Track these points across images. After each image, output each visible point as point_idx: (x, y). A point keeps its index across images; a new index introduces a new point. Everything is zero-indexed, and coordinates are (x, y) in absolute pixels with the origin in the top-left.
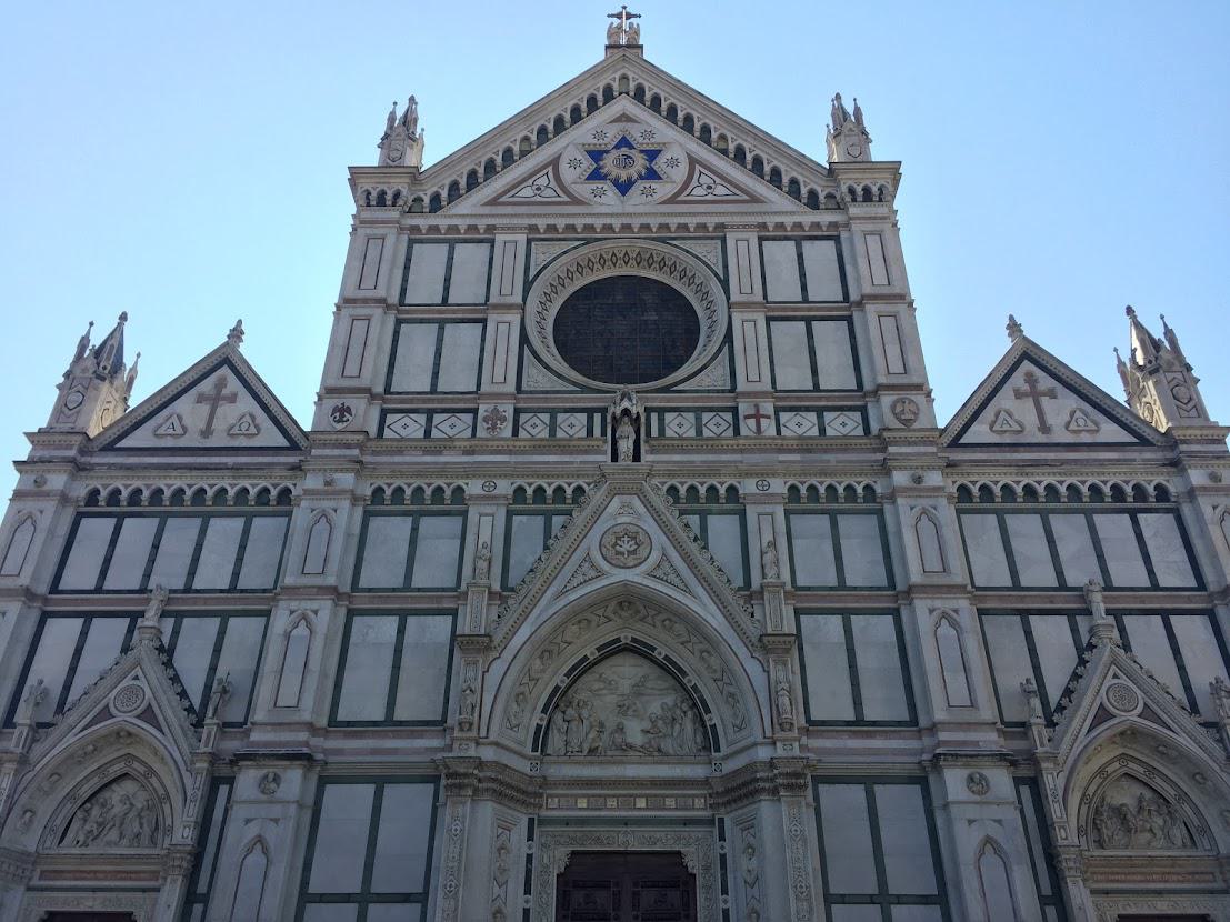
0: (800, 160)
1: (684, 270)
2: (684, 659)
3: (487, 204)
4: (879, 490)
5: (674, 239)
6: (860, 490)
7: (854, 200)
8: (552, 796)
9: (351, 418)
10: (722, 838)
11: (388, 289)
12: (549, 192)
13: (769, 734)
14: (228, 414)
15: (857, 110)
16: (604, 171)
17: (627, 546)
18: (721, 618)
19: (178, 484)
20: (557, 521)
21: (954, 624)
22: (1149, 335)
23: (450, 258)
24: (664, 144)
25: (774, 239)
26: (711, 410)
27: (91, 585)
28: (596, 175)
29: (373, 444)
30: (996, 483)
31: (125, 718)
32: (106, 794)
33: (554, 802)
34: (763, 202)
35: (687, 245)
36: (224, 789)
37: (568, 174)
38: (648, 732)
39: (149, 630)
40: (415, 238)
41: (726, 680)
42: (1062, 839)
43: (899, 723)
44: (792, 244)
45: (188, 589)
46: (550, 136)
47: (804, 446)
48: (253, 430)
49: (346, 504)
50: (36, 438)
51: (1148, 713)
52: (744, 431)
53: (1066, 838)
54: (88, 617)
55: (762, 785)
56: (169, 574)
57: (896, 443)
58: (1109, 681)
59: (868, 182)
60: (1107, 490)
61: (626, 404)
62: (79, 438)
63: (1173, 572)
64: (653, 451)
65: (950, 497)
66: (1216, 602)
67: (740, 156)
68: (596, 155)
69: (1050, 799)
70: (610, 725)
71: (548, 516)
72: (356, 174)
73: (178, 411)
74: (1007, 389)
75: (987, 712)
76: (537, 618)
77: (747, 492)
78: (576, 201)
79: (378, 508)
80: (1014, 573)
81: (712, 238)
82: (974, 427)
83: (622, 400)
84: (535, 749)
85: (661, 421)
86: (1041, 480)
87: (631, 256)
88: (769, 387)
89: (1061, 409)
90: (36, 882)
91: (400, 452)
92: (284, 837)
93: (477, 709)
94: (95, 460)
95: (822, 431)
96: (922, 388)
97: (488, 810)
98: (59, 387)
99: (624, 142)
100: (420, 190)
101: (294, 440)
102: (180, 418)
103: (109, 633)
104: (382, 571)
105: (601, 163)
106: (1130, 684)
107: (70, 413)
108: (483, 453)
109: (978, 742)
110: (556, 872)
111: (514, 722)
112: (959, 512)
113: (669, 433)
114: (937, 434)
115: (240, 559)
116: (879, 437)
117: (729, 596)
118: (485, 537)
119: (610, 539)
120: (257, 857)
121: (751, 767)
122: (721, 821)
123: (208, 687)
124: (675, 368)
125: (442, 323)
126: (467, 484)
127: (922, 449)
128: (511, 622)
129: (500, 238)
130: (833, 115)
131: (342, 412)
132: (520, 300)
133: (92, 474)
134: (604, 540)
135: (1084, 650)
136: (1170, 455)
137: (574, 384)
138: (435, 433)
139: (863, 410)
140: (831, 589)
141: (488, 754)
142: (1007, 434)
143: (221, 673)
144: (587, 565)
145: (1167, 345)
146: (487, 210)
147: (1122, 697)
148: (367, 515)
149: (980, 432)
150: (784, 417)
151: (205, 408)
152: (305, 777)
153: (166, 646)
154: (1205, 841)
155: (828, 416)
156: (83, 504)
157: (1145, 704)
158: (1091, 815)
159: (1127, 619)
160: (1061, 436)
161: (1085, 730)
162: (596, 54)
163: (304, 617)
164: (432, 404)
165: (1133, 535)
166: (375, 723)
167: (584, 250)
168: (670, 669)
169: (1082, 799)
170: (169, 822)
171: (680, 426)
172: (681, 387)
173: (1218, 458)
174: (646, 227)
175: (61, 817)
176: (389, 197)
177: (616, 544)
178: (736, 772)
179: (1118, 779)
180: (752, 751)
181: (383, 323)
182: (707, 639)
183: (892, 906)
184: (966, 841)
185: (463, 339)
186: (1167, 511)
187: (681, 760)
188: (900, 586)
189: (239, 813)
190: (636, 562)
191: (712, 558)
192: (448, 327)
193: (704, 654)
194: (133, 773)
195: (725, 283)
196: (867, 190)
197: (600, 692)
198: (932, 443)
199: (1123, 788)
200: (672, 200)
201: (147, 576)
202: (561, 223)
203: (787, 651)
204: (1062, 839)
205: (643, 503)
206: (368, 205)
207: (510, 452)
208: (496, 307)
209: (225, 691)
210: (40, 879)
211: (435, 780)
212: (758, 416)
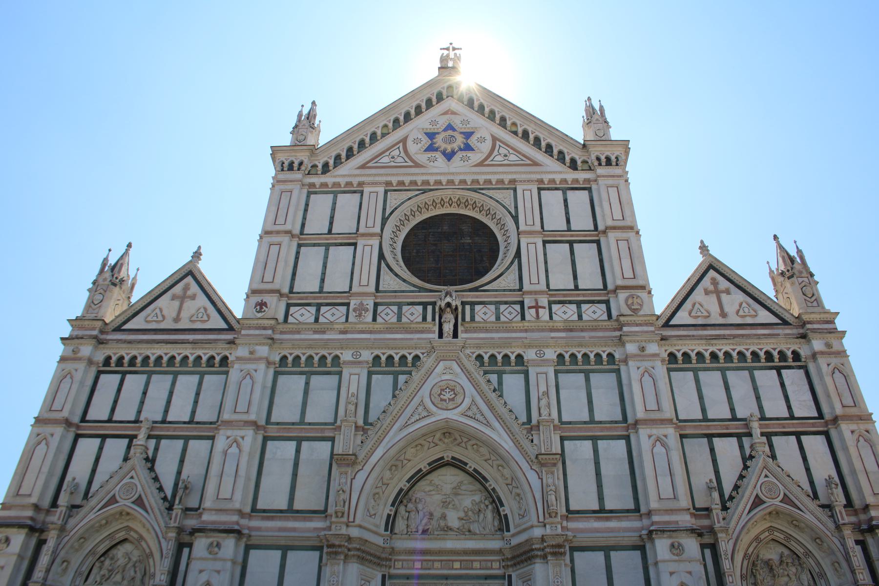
0: (565, 138)
1: (489, 209)
3: (359, 168)
5: (482, 189)
6: (604, 356)
7: (600, 164)
8: (399, 560)
11: (293, 224)
12: (400, 160)
13: (541, 519)
14: (190, 307)
15: (602, 108)
16: (436, 145)
17: (448, 395)
18: (511, 444)
19: (159, 352)
20: (402, 378)
22: (788, 254)
23: (334, 203)
24: (476, 128)
25: (548, 189)
26: (506, 303)
27: (106, 418)
28: (431, 148)
29: (280, 327)
30: (692, 351)
31: (125, 503)
33: (399, 565)
34: (541, 165)
35: (490, 193)
36: (186, 551)
37: (412, 148)
38: (462, 519)
39: (141, 447)
41: (514, 484)
42: (730, 583)
43: (628, 511)
45: (164, 421)
48: (205, 318)
49: (262, 366)
50: (74, 323)
51: (786, 500)
52: (527, 317)
53: (733, 582)
54: (104, 437)
55: (536, 553)
56: (153, 411)
58: (762, 479)
59: (608, 153)
60: (762, 354)
61: (448, 299)
62: (100, 323)
63: (803, 407)
64: (466, 331)
65: (663, 361)
66: (829, 426)
67: (525, 135)
68: (431, 136)
69: (723, 557)
70: (437, 514)
71: (396, 375)
72: (275, 151)
74: (700, 289)
75: (684, 502)
76: (387, 444)
77: (530, 358)
78: (417, 165)
79: (283, 369)
80: (704, 410)
81: (508, 189)
82: (679, 314)
83: (446, 296)
84: (386, 530)
86: (721, 348)
87: (453, 200)
88: (544, 288)
89: (734, 300)
91: (299, 332)
93: (347, 504)
94: (109, 337)
95: (580, 317)
96: (644, 288)
97: (354, 569)
98: (89, 290)
99: (450, 127)
100: (317, 160)
101: (231, 326)
102: (161, 310)
103: (115, 448)
105: (434, 140)
106: (775, 481)
109: (677, 521)
111: (372, 512)
112: (669, 370)
113: (477, 318)
114: (655, 318)
115: (196, 402)
116: (617, 320)
117: (516, 428)
118: (353, 389)
119: (437, 390)
122: (510, 577)
123: (176, 485)
125: (327, 246)
126: (342, 354)
127: (645, 328)
128: (370, 446)
129: (367, 190)
130: (586, 110)
131: (262, 305)
132: (377, 229)
133: (107, 346)
134: (433, 391)
135: (747, 459)
136: (801, 331)
137: (414, 286)
138: (321, 319)
139: (607, 302)
140: (585, 423)
141: (354, 532)
142: (700, 318)
143: (184, 476)
145: (798, 260)
146: (358, 172)
147: (770, 490)
148: (277, 374)
149: (682, 318)
150: (555, 307)
151: (177, 303)
152: (237, 545)
155: (584, 307)
156: (101, 365)
159: (774, 439)
163: (236, 441)
165: (778, 384)
166: (281, 511)
167: (423, 197)
168: (478, 477)
169: (744, 557)
171: (485, 313)
173: (830, 333)
174: (464, 182)
177: (441, 394)
178: (519, 545)
180: (531, 530)
181: (289, 246)
185: (341, 256)
186: (800, 367)
187: (484, 537)
188: (630, 420)
189: (195, 566)
190: (454, 406)
191: (505, 403)
192: (332, 249)
193: (500, 468)
194: (131, 538)
195: (516, 219)
196: (608, 160)
197: (430, 493)
198: (651, 324)
199: (771, 549)
200: (481, 164)
201: (139, 412)
202: (407, 180)
204: (730, 583)
205: (459, 366)
206: (282, 170)
207: (371, 332)
208: (363, 235)
209: (186, 488)
211: (320, 548)
212: (537, 307)
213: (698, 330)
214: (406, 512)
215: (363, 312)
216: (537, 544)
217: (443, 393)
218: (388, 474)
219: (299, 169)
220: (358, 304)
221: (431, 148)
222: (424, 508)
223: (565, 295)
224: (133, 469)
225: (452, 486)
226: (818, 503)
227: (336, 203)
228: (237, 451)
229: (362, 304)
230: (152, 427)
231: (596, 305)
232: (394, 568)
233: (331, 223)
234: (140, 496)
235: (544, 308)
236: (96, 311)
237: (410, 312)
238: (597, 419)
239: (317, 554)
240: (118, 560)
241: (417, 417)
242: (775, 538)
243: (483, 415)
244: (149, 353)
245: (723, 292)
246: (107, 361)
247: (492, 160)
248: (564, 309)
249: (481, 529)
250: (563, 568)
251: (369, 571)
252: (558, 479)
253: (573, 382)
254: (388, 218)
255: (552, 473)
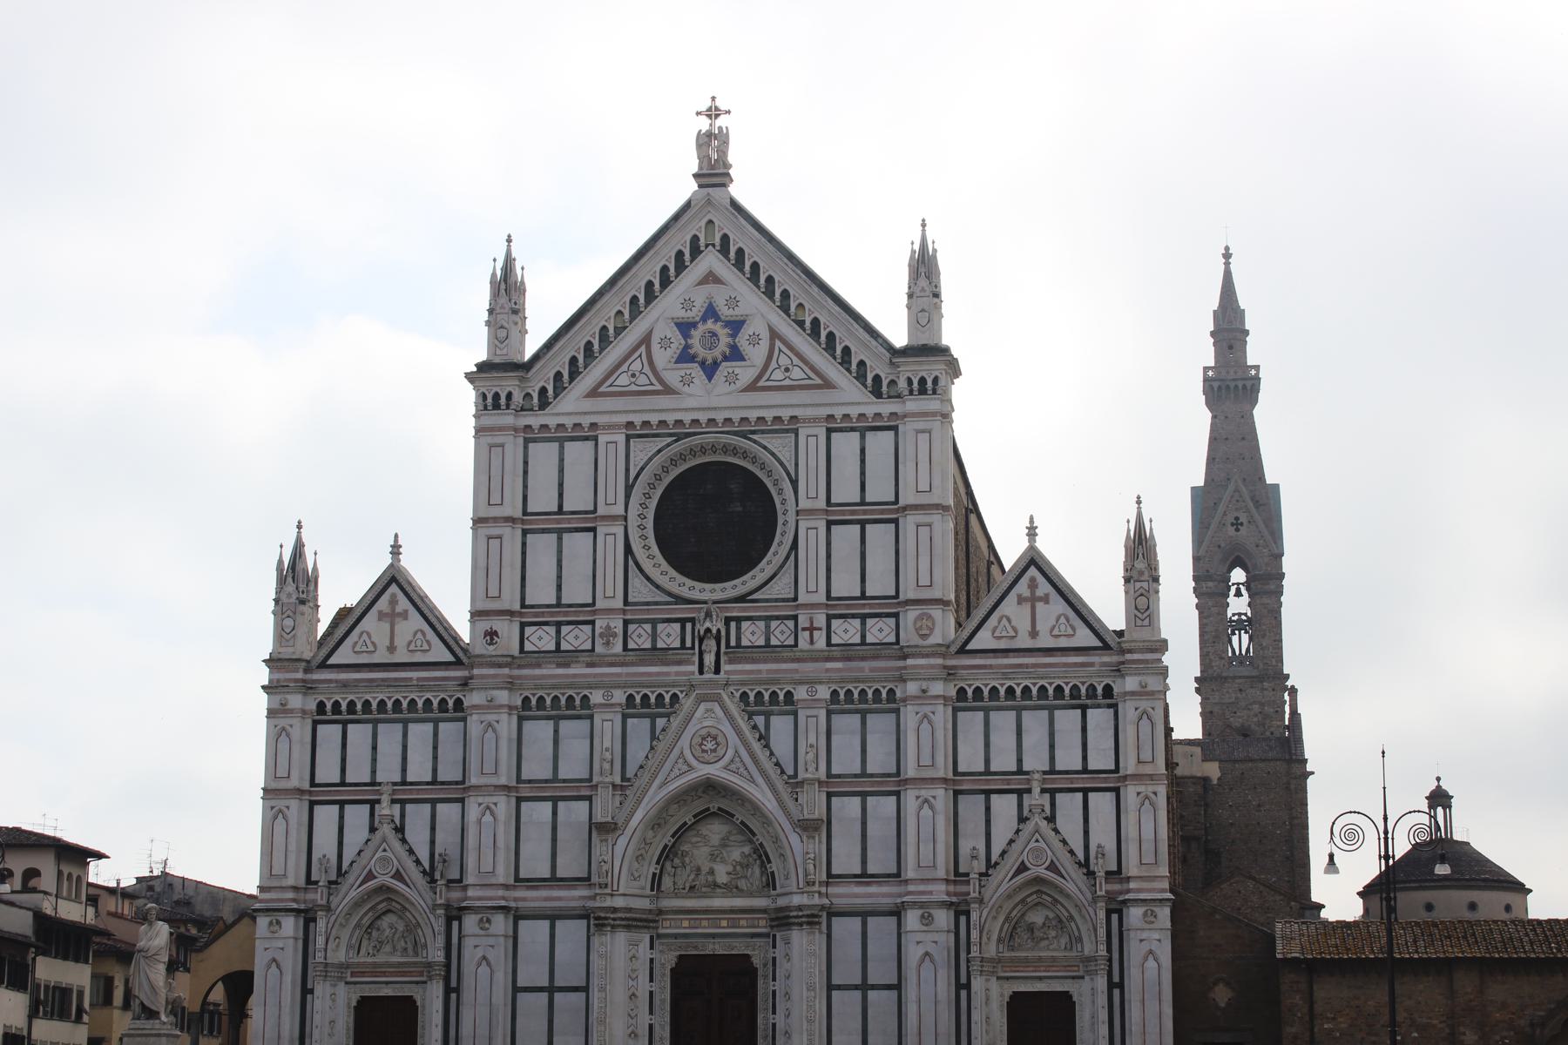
2: (754, 824)
4: (899, 694)
5: (754, 432)
7: (911, 393)
8: (666, 919)
9: (499, 640)
10: (774, 947)
12: (642, 380)
17: (709, 745)
18: (775, 803)
19: (381, 696)
20: (660, 722)
21: (931, 807)
23: (561, 460)
24: (747, 316)
26: (777, 618)
28: (685, 357)
32: (379, 922)
33: (667, 924)
34: (834, 387)
36: (455, 924)
37: (662, 357)
38: (730, 874)
40: (530, 437)
43: (889, 876)
44: (857, 435)
45: (404, 783)
46: (642, 309)
47: (847, 652)
48: (426, 647)
49: (504, 717)
51: (1052, 867)
52: (803, 643)
56: (388, 772)
57: (913, 656)
59: (924, 374)
61: (708, 624)
62: (304, 664)
64: (731, 662)
68: (685, 327)
70: (705, 869)
73: (366, 629)
74: (1012, 596)
76: (647, 804)
78: (668, 390)
80: (987, 761)
81: (787, 431)
83: (705, 619)
84: (652, 890)
85: (738, 628)
90: (349, 979)
91: (539, 666)
92: (499, 955)
93: (610, 875)
94: (316, 676)
95: (863, 637)
97: (621, 937)
99: (711, 312)
101: (460, 656)
103: (357, 816)
104: (537, 767)
105: (690, 341)
107: (289, 636)
108: (600, 666)
110: (670, 967)
111: (636, 875)
112: (955, 710)
113: (745, 642)
115: (435, 758)
117: (780, 785)
119: (697, 740)
120: (484, 969)
121: (788, 908)
122: (774, 936)
124: (750, 563)
126: (591, 693)
129: (602, 439)
131: (492, 635)
132: (622, 512)
135: (1022, 819)
137: (670, 594)
140: (856, 776)
141: (619, 902)
142: (1004, 639)
143: (438, 851)
144: (681, 761)
146: (588, 405)
148: (521, 719)
150: (835, 623)
151: (386, 626)
152: (506, 917)
153: (399, 826)
154: (1079, 945)
155: (870, 622)
157: (1052, 861)
158: (1010, 931)
160: (1045, 641)
161: (1008, 878)
162: (687, 188)
163: (488, 808)
164: (560, 614)
169: (1007, 919)
170: (423, 941)
172: (754, 596)
174: (728, 421)
175: (355, 938)
176: (503, 401)
178: (781, 909)
179: (1036, 905)
180: (790, 896)
182: (763, 815)
183: (869, 992)
184: (913, 954)
185: (577, 545)
186: (1109, 706)
187: (751, 895)
189: (468, 943)
190: (716, 759)
191: (772, 754)
192: (566, 536)
194: (393, 909)
195: (794, 483)
196: (923, 381)
200: (752, 387)
201: (374, 772)
202: (654, 419)
203: (817, 829)
206: (485, 408)
208: (604, 518)
210: (352, 976)
211: (586, 916)
212: (811, 629)
213: (998, 658)
214: (673, 867)
215: (611, 639)
216: (796, 910)
217: (705, 743)
218: (650, 834)
219: (508, 407)
220: (604, 626)
221: (685, 357)
222: (691, 862)
223: (848, 606)
224: (384, 840)
225: (721, 836)
226: (1085, 871)
227: (563, 460)
228: (491, 819)
229: (608, 627)
230: (394, 790)
231: (883, 619)
232: (663, 928)
233: (561, 495)
234: (398, 870)
235: (820, 629)
236: (291, 643)
237: (665, 632)
238: (869, 771)
239: (585, 922)
240: (384, 930)
241: (676, 772)
242: (1041, 900)
243: (746, 769)
244: (368, 697)
245: (1040, 599)
246: (321, 707)
247: (768, 380)
248: (847, 625)
249: (749, 885)
250: (817, 934)
251: (635, 935)
252: (820, 842)
253: (847, 724)
254: (633, 485)
255: (814, 838)
